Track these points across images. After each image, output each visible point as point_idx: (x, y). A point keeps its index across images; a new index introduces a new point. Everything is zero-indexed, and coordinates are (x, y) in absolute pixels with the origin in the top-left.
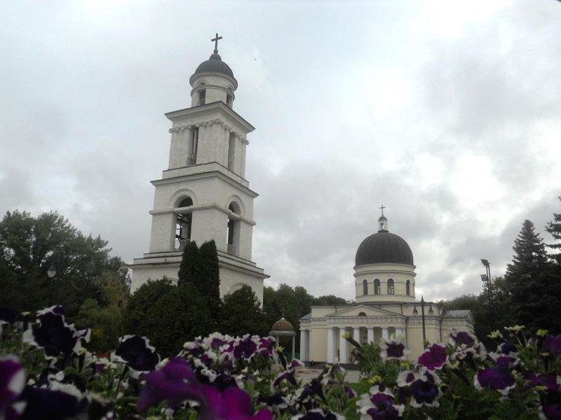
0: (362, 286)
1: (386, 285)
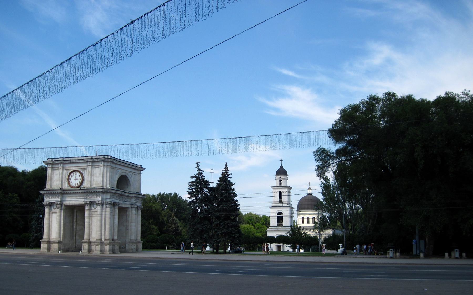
0: (302, 219)
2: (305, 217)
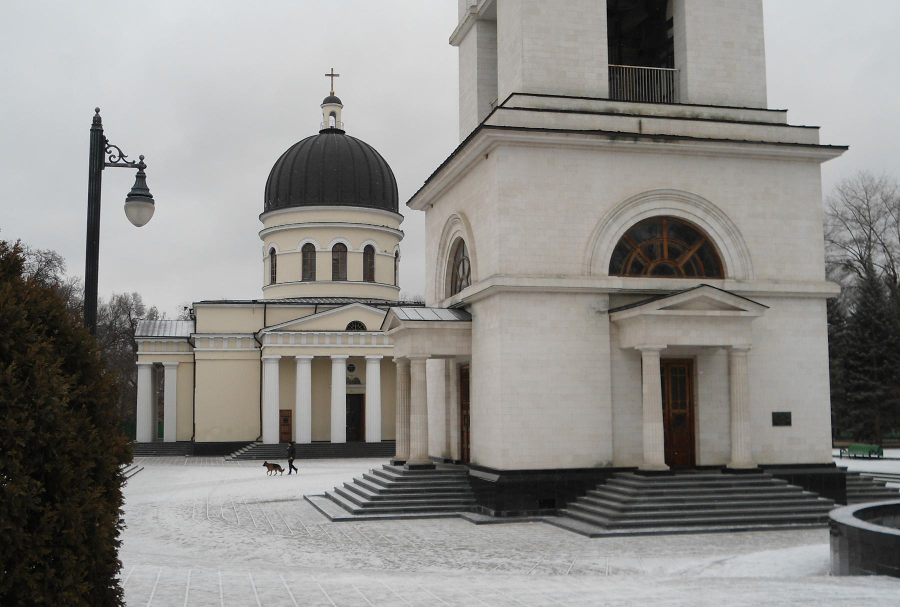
0: (299, 258)
1: (360, 259)
2: (324, 245)
